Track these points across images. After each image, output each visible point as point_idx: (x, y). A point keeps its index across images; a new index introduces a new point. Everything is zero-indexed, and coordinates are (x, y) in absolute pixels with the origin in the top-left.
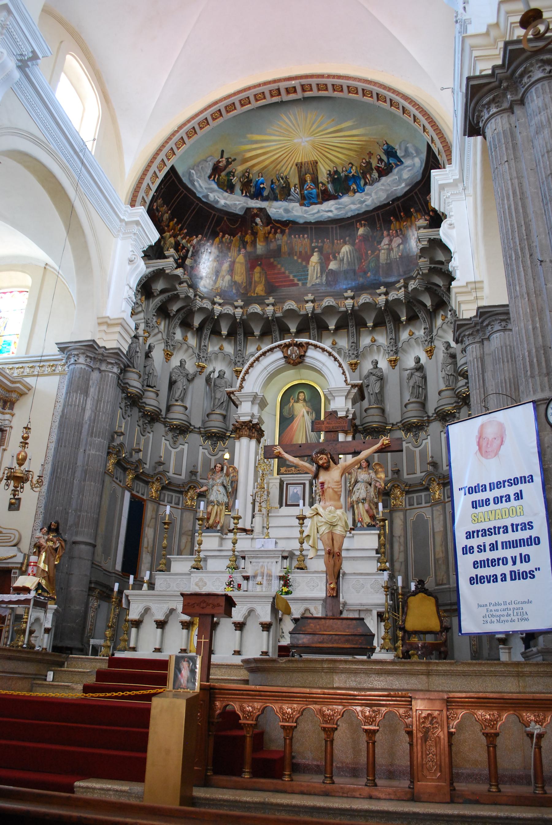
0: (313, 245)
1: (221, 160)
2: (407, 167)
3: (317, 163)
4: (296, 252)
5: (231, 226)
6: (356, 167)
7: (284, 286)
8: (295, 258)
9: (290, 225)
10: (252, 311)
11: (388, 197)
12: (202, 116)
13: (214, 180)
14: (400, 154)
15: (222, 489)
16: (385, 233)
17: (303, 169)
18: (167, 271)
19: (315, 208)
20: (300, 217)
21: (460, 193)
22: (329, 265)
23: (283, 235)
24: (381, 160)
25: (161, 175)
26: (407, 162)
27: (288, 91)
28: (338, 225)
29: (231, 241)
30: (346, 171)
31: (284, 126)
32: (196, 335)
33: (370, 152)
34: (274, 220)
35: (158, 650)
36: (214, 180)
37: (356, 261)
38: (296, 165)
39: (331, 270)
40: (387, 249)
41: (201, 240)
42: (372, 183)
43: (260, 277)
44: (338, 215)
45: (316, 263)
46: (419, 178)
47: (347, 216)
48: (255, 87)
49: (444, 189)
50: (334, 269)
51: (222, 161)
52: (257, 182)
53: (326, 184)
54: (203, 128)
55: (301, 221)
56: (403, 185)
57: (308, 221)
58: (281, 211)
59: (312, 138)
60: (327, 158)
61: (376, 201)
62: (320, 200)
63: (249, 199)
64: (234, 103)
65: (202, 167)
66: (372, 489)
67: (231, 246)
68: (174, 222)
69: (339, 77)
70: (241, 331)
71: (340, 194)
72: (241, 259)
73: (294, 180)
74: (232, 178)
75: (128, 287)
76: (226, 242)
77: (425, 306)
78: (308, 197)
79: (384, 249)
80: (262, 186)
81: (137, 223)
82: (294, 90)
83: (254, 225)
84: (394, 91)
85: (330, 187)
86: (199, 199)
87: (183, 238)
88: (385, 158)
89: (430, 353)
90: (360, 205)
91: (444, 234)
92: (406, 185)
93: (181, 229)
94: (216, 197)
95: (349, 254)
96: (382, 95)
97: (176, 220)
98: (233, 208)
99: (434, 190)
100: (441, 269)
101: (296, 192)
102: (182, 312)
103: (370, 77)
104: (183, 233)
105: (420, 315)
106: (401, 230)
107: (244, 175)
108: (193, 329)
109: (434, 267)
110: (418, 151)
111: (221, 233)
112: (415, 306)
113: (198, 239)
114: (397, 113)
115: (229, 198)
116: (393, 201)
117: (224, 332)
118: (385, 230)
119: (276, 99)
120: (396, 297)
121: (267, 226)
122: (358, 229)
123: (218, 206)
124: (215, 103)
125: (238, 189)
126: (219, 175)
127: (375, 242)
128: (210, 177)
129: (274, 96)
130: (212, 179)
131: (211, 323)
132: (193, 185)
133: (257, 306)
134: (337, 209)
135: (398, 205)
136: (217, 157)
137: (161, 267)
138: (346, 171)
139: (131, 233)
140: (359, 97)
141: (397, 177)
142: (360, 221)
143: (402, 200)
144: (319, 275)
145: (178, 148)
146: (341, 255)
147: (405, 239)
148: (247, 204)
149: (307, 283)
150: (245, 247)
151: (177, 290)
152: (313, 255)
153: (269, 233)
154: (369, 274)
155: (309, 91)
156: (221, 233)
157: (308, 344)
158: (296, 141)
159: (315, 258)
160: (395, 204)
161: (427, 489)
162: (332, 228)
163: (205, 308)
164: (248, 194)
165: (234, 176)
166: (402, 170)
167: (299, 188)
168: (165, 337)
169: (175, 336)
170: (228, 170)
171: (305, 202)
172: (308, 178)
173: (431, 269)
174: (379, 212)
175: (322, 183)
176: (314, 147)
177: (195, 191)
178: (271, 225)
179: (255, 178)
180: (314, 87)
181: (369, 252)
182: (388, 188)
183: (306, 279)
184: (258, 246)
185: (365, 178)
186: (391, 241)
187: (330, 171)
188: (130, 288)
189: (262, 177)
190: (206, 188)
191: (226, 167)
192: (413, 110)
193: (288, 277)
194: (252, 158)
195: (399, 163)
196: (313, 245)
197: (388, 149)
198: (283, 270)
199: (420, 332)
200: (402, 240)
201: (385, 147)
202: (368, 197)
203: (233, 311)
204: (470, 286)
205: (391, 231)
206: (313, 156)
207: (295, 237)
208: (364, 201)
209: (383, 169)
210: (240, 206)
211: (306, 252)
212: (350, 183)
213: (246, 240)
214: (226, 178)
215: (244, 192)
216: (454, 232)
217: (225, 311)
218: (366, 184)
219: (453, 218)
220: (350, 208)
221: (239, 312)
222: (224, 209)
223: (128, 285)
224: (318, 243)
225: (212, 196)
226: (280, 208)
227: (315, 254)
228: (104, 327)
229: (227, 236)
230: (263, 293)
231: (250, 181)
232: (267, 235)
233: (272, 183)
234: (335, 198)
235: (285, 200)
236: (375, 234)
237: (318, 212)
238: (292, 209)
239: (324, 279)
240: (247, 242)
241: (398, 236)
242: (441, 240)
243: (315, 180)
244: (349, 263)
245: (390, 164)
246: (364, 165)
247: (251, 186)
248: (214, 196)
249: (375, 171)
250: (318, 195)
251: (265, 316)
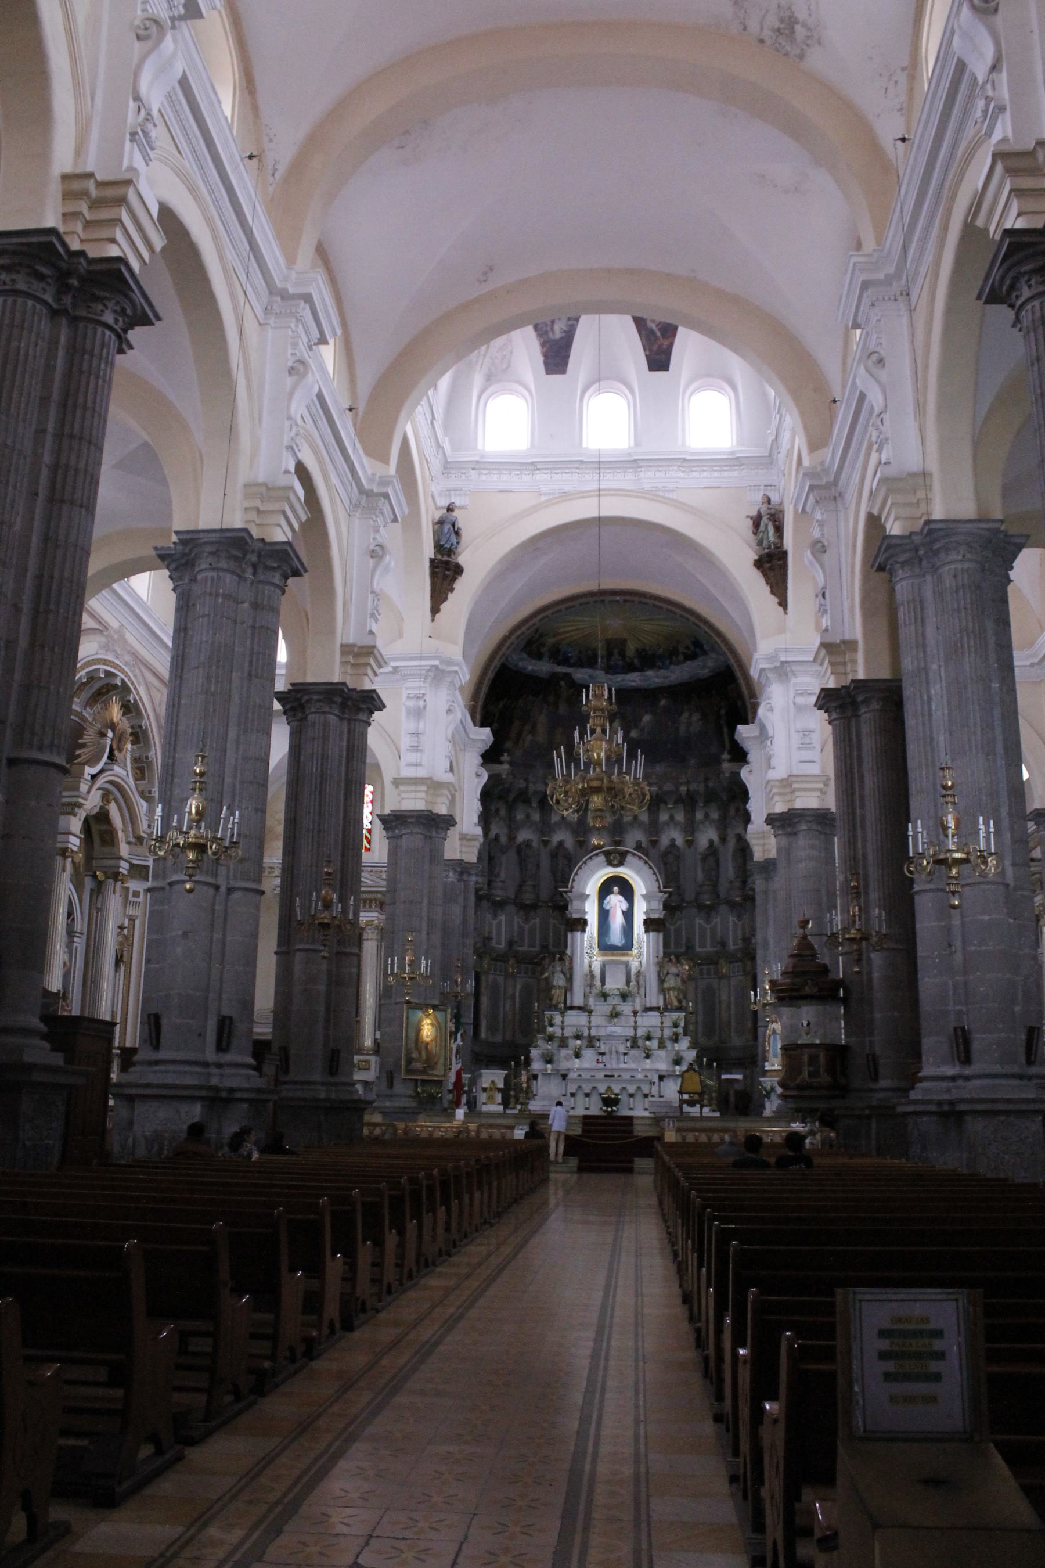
14: (706, 647)
15: (562, 976)
35: (587, 1109)
42: (678, 663)
58: (586, 677)
66: (679, 979)
85: (636, 661)
89: (723, 839)
125: (546, 658)
146: (642, 724)
157: (627, 852)
161: (716, 963)
172: (616, 651)
194: (565, 632)
199: (715, 815)
208: (667, 677)
218: (671, 663)
225: (521, 664)
228: (465, 842)
231: (558, 650)
233: (580, 652)
237: (623, 680)
243: (622, 654)
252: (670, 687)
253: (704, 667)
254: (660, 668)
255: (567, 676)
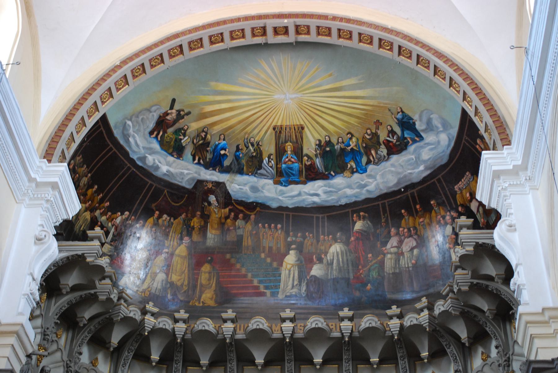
0: (289, 239)
1: (169, 111)
2: (428, 144)
3: (303, 128)
4: (264, 248)
5: (173, 204)
6: (357, 139)
7: (245, 295)
8: (263, 256)
9: (258, 209)
10: (200, 328)
11: (398, 183)
12: (156, 51)
13: (156, 137)
14: (419, 126)
16: (393, 231)
17: (283, 135)
18: (88, 260)
19: (295, 189)
20: (273, 199)
21: (521, 185)
22: (311, 269)
23: (246, 223)
24: (392, 132)
25: (90, 123)
26: (429, 138)
27: (276, 31)
28: (326, 215)
29: (170, 225)
30: (343, 142)
31: (263, 76)
32: (109, 359)
33: (378, 121)
34: (234, 200)
36: (156, 137)
37: (350, 268)
38: (274, 129)
39: (315, 276)
40: (395, 253)
41: (127, 219)
42: (379, 161)
43: (209, 280)
44: (326, 201)
45: (293, 265)
46: (445, 160)
47: (340, 203)
48: (232, 21)
49: (499, 177)
50: (318, 276)
51: (171, 113)
52: (217, 146)
53: (314, 158)
54: (155, 66)
55: (274, 205)
56: (422, 168)
57: (284, 205)
58: (247, 188)
59: (299, 95)
60: (318, 123)
61: (381, 186)
62: (303, 179)
63: (202, 168)
64: (201, 39)
65: (142, 119)
67: (169, 232)
68: (94, 189)
69: (348, 20)
70: (179, 357)
71: (332, 173)
72: (182, 250)
73: (269, 148)
74: (182, 137)
75: (31, 278)
76: (163, 225)
77: (457, 338)
78: (287, 174)
79: (391, 253)
80: (222, 152)
81: (54, 186)
82: (286, 31)
83: (206, 204)
84: (424, 46)
85: (318, 162)
86: (132, 161)
87: (102, 214)
88: (398, 130)
90: (358, 190)
91: (502, 238)
92: (426, 169)
93: (102, 201)
94: (157, 161)
95: (340, 256)
96: (406, 49)
97: (96, 187)
98: (178, 179)
99: (484, 178)
100: (487, 286)
101: (270, 164)
102: (97, 321)
103: (390, 24)
104: (103, 207)
105: (448, 351)
106: (415, 228)
107: (198, 135)
108: (108, 349)
109: (478, 283)
110: (446, 125)
111: (157, 212)
112: (442, 337)
113: (124, 217)
114: (427, 75)
115: (174, 165)
116: (406, 188)
117: (155, 357)
118: (392, 227)
119: (259, 40)
120: (415, 322)
121: (225, 208)
122: (354, 223)
123: (158, 174)
124: (176, 36)
126: (165, 132)
127: (379, 243)
128: (151, 133)
129: (257, 36)
130: (154, 135)
131: (137, 342)
132: (128, 141)
133: (209, 321)
134: (325, 193)
135: (412, 195)
136: (165, 107)
137: (80, 253)
138: (343, 142)
139: (42, 199)
140: (374, 48)
141: (413, 157)
142: (358, 212)
143: (419, 188)
144: (296, 283)
145: (118, 90)
147: (422, 242)
148: (199, 175)
149: (278, 293)
150: (189, 234)
151: (96, 289)
152: (289, 254)
153: (227, 218)
154: (369, 286)
155: (305, 34)
156: (157, 212)
158: (276, 97)
159: (291, 259)
160: (409, 193)
162: (318, 218)
163: (131, 318)
164: (201, 161)
165: (184, 135)
166: (422, 147)
167: (274, 159)
168: (65, 358)
169: (81, 357)
170: (177, 126)
171: (282, 179)
172: (289, 147)
173: (473, 287)
174: (386, 201)
175: (307, 155)
176: (301, 107)
177: (128, 149)
178: (230, 207)
179: (214, 141)
180: (313, 30)
181: (370, 255)
182: (400, 170)
183: (278, 287)
184: (209, 235)
185: (368, 154)
186: (401, 242)
187: (320, 141)
188: (34, 279)
189: (224, 140)
190: (144, 148)
191: (175, 122)
192: (450, 72)
193: (251, 281)
195: (417, 139)
196: (289, 239)
197: (403, 118)
198: (243, 271)
200: (417, 242)
201: (400, 116)
202: (370, 180)
203: (172, 326)
204: (547, 314)
205: (401, 229)
206: (298, 119)
207: (264, 227)
208: (365, 186)
209: (395, 145)
210: (189, 177)
211: (278, 249)
212: (347, 159)
213: (192, 224)
214: (173, 137)
215: (197, 158)
216: (516, 237)
217: (161, 326)
218: (369, 162)
219: (513, 217)
220: (345, 192)
221: (181, 327)
222: (166, 178)
223: (32, 274)
224: (297, 237)
225: (150, 159)
226: (245, 185)
227: (292, 252)
229: (165, 216)
230: (212, 303)
232: (223, 221)
233: (238, 149)
234: (325, 177)
235: (254, 174)
236: (378, 231)
237: (299, 194)
238: (263, 188)
239: (304, 288)
240: (193, 228)
241: (411, 236)
242: (493, 246)
243: (298, 152)
244: (340, 270)
245: (406, 138)
246: (368, 137)
247: (207, 151)
248: (154, 160)
249: (383, 146)
250: (300, 172)
251: (220, 337)
252: (367, 201)
253: (417, 162)
254: (353, 173)
255: (219, 185)
